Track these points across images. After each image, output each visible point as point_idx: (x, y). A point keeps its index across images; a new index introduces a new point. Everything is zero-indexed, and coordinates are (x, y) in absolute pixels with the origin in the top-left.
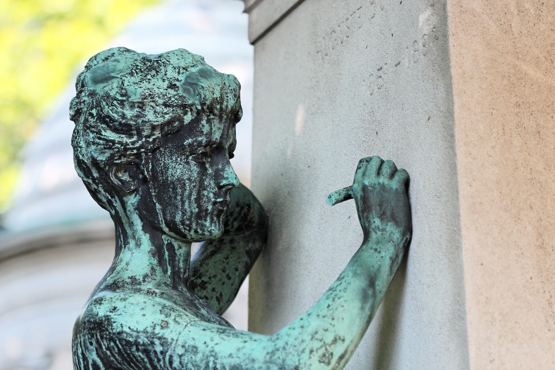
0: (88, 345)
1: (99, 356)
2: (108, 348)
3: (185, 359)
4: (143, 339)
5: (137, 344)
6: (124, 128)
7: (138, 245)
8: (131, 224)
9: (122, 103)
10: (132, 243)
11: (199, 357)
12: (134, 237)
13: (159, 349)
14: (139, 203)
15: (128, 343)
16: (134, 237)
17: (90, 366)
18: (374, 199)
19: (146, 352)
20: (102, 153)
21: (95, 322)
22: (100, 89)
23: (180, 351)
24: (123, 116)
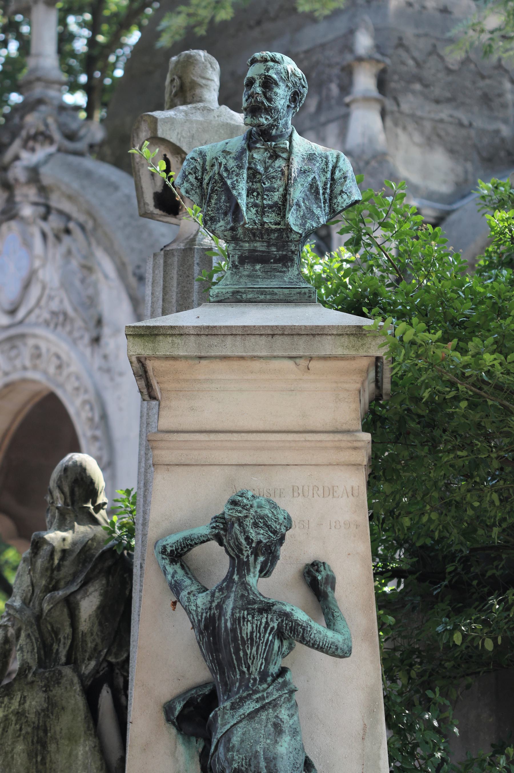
0: (275, 620)
1: (278, 625)
2: (286, 624)
3: (316, 635)
4: (304, 625)
5: (302, 626)
6: (275, 532)
7: (254, 576)
8: (255, 567)
9: (276, 522)
10: (252, 575)
11: (321, 636)
12: (254, 573)
13: (309, 629)
14: (264, 561)
15: (299, 625)
16: (254, 573)
17: (269, 628)
18: (330, 580)
19: (304, 630)
20: (265, 539)
21: (285, 613)
22: (259, 510)
23: (315, 632)
24: (276, 527)
